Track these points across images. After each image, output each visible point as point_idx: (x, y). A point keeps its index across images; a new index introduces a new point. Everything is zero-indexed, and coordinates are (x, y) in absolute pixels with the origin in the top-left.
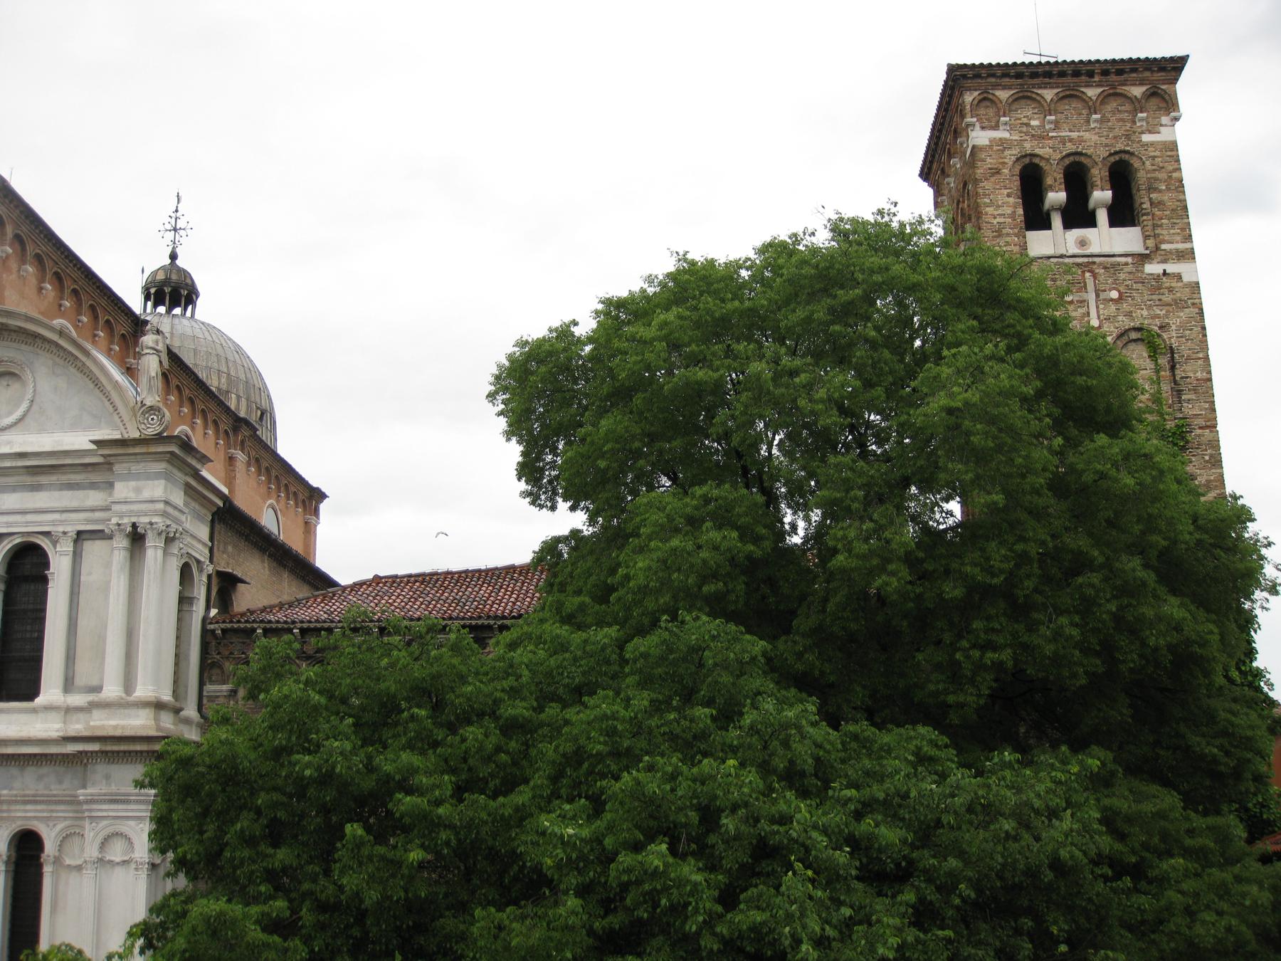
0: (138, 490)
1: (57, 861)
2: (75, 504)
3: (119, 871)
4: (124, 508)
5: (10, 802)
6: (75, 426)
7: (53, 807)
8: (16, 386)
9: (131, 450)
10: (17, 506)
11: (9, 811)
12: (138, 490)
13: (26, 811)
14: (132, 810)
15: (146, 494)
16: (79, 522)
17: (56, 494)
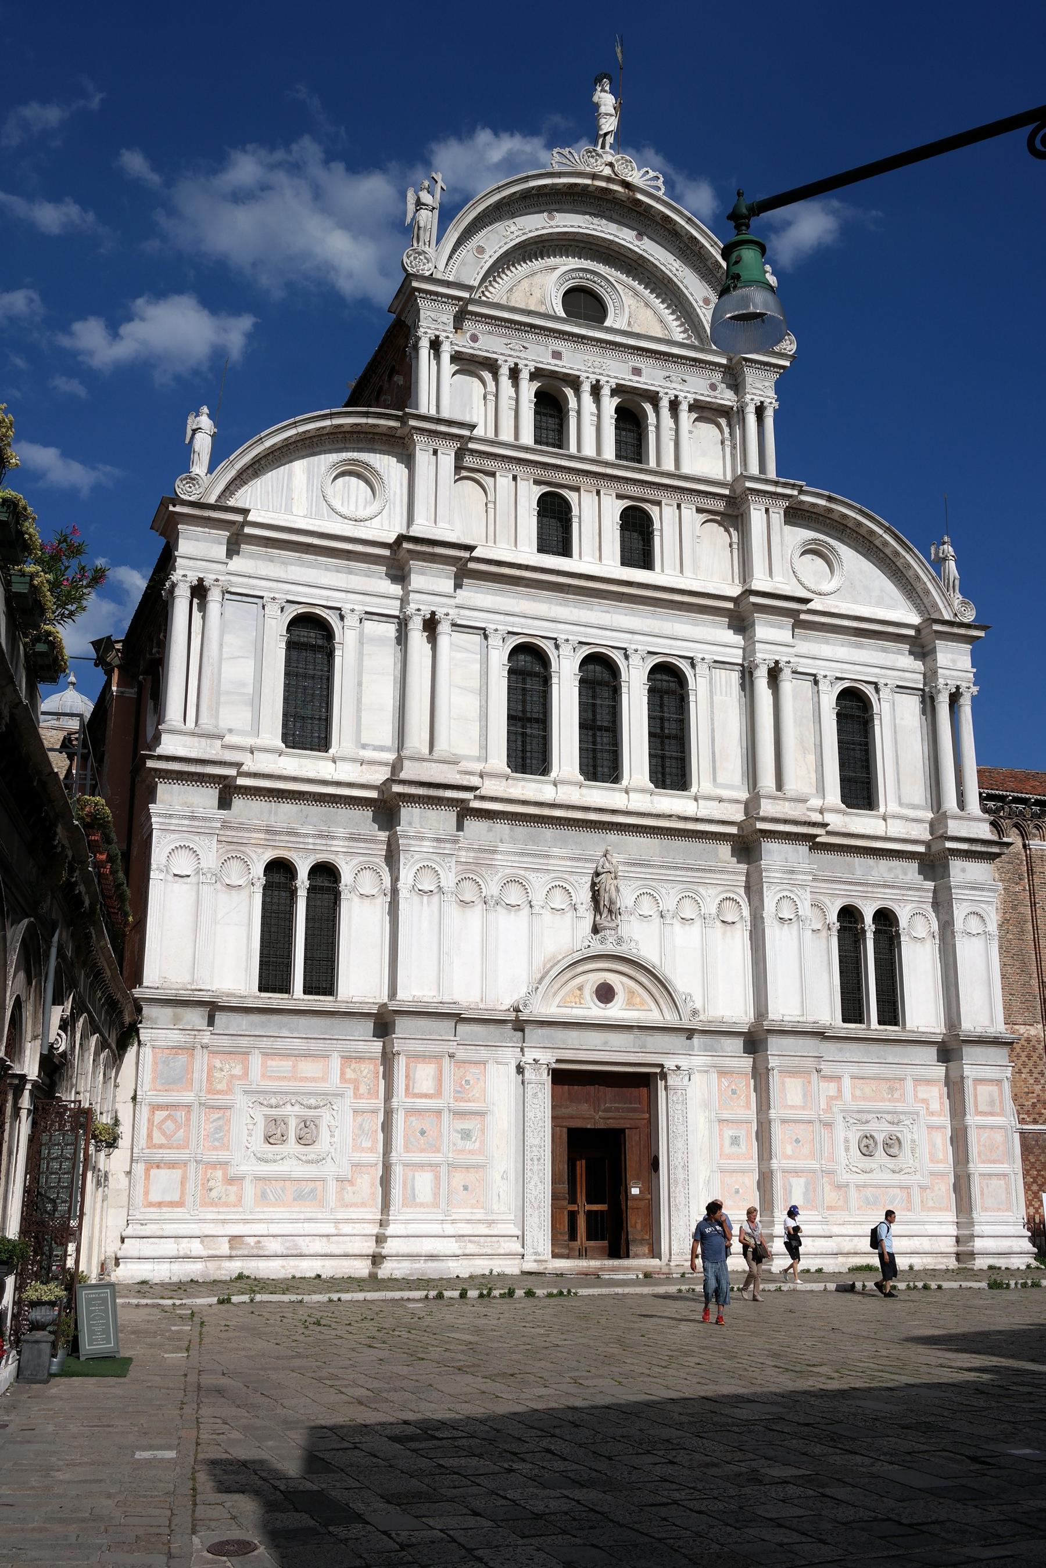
0: (954, 661)
1: (909, 934)
2: (889, 664)
3: (974, 938)
4: (947, 672)
5: (874, 885)
6: (880, 603)
7: (905, 892)
8: (819, 561)
9: (956, 630)
10: (847, 658)
11: (873, 892)
12: (954, 661)
13: (885, 893)
14: (985, 896)
15: (959, 666)
16: (892, 679)
17: (875, 653)
